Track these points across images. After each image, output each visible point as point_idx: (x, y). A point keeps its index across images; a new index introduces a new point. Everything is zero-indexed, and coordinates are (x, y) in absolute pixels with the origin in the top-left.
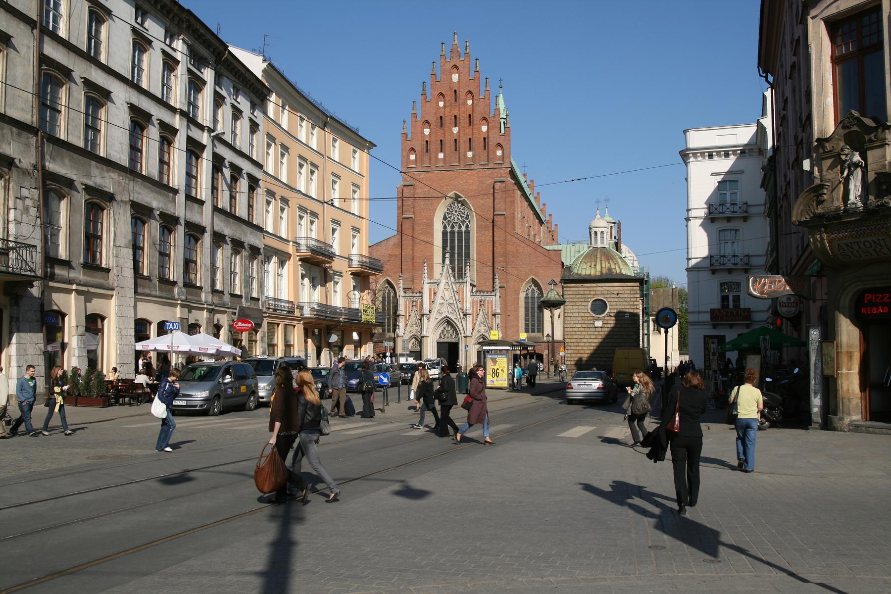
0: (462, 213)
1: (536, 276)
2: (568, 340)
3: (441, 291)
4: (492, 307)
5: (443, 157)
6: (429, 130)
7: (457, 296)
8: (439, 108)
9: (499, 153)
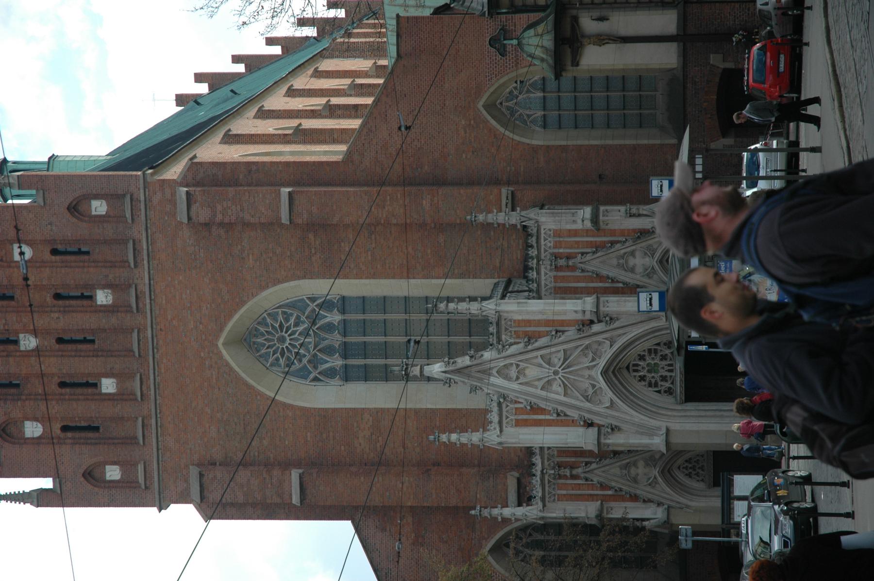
0: (287, 320)
4: (575, 233)
5: (114, 380)
6: (28, 424)
9: (99, 207)
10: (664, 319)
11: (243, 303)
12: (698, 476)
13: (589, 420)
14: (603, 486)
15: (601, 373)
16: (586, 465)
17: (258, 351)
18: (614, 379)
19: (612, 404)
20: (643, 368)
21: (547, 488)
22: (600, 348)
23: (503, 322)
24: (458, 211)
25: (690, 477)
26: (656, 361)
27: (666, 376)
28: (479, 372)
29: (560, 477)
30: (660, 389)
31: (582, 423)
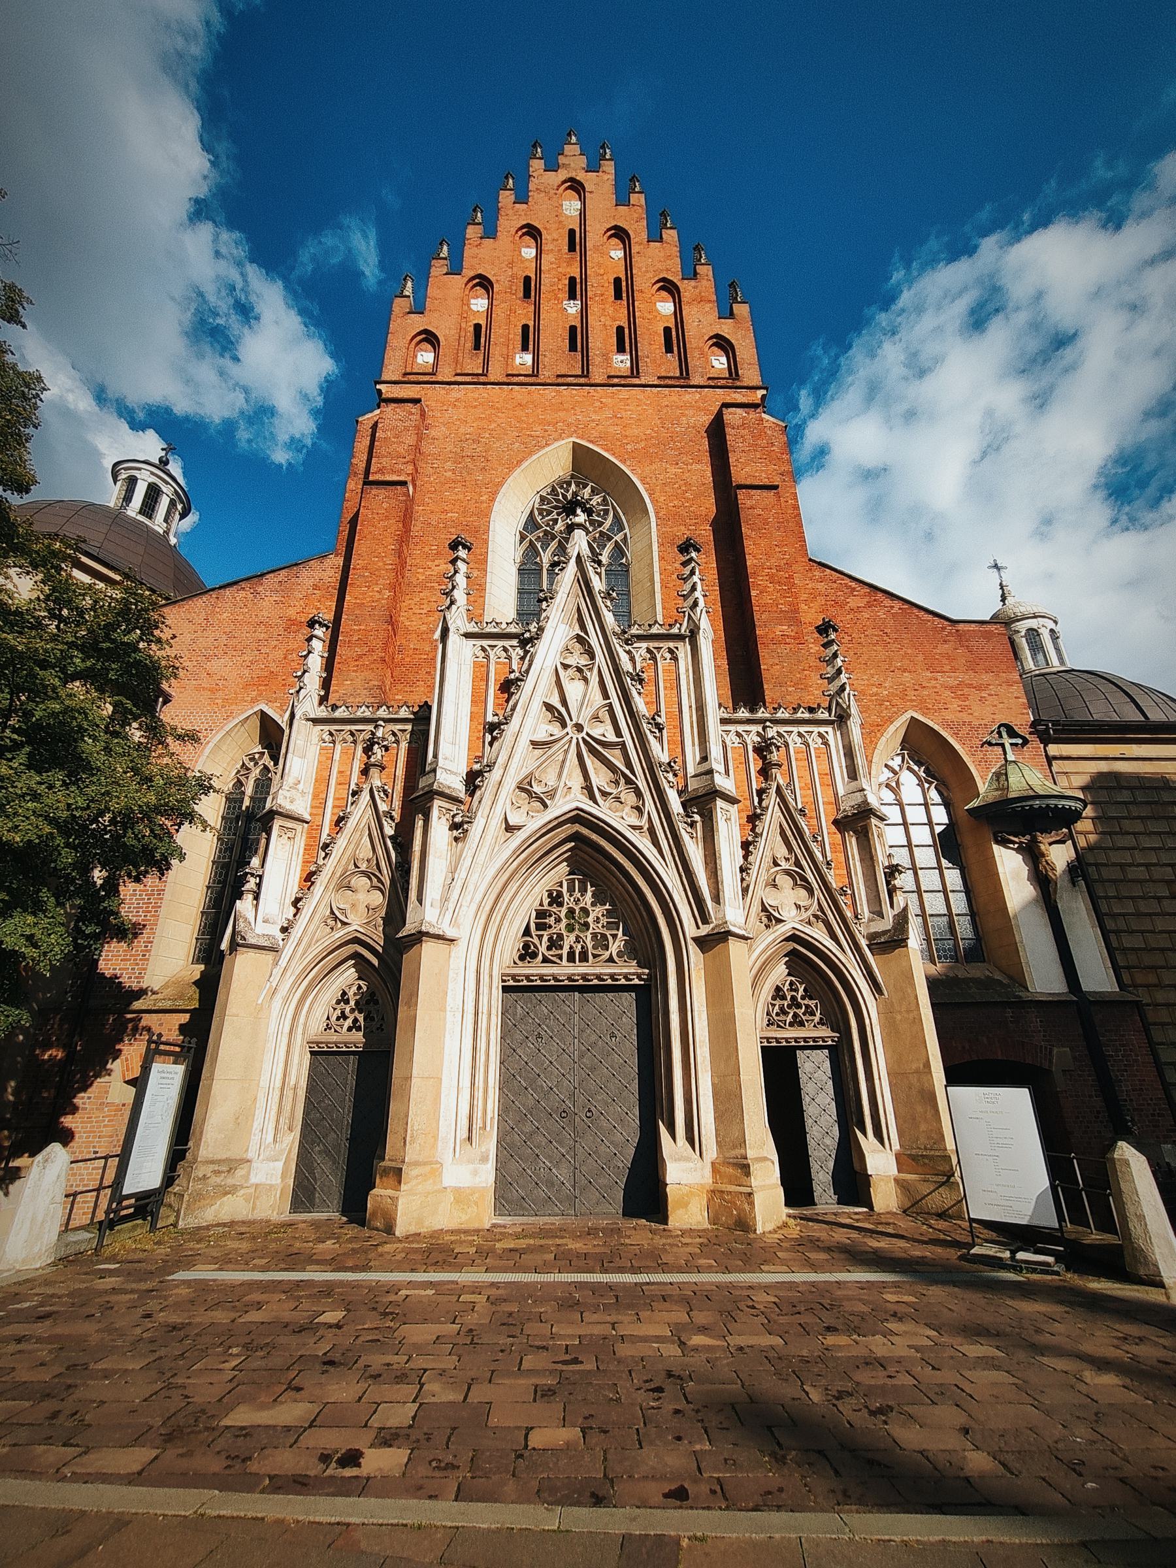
1: (925, 711)
2: (1144, 997)
3: (547, 679)
7: (640, 704)
8: (523, 260)
10: (705, 930)
11: (624, 462)
12: (338, 1019)
13: (482, 781)
14: (340, 822)
15: (577, 809)
16: (385, 791)
17: (562, 487)
18: (563, 836)
19: (509, 828)
20: (577, 901)
21: (348, 727)
22: (627, 809)
23: (671, 645)
24: (778, 667)
25: (338, 1002)
26: (591, 925)
27: (561, 948)
28: (579, 607)
29: (368, 750)
30: (533, 934)
31: (477, 767)
